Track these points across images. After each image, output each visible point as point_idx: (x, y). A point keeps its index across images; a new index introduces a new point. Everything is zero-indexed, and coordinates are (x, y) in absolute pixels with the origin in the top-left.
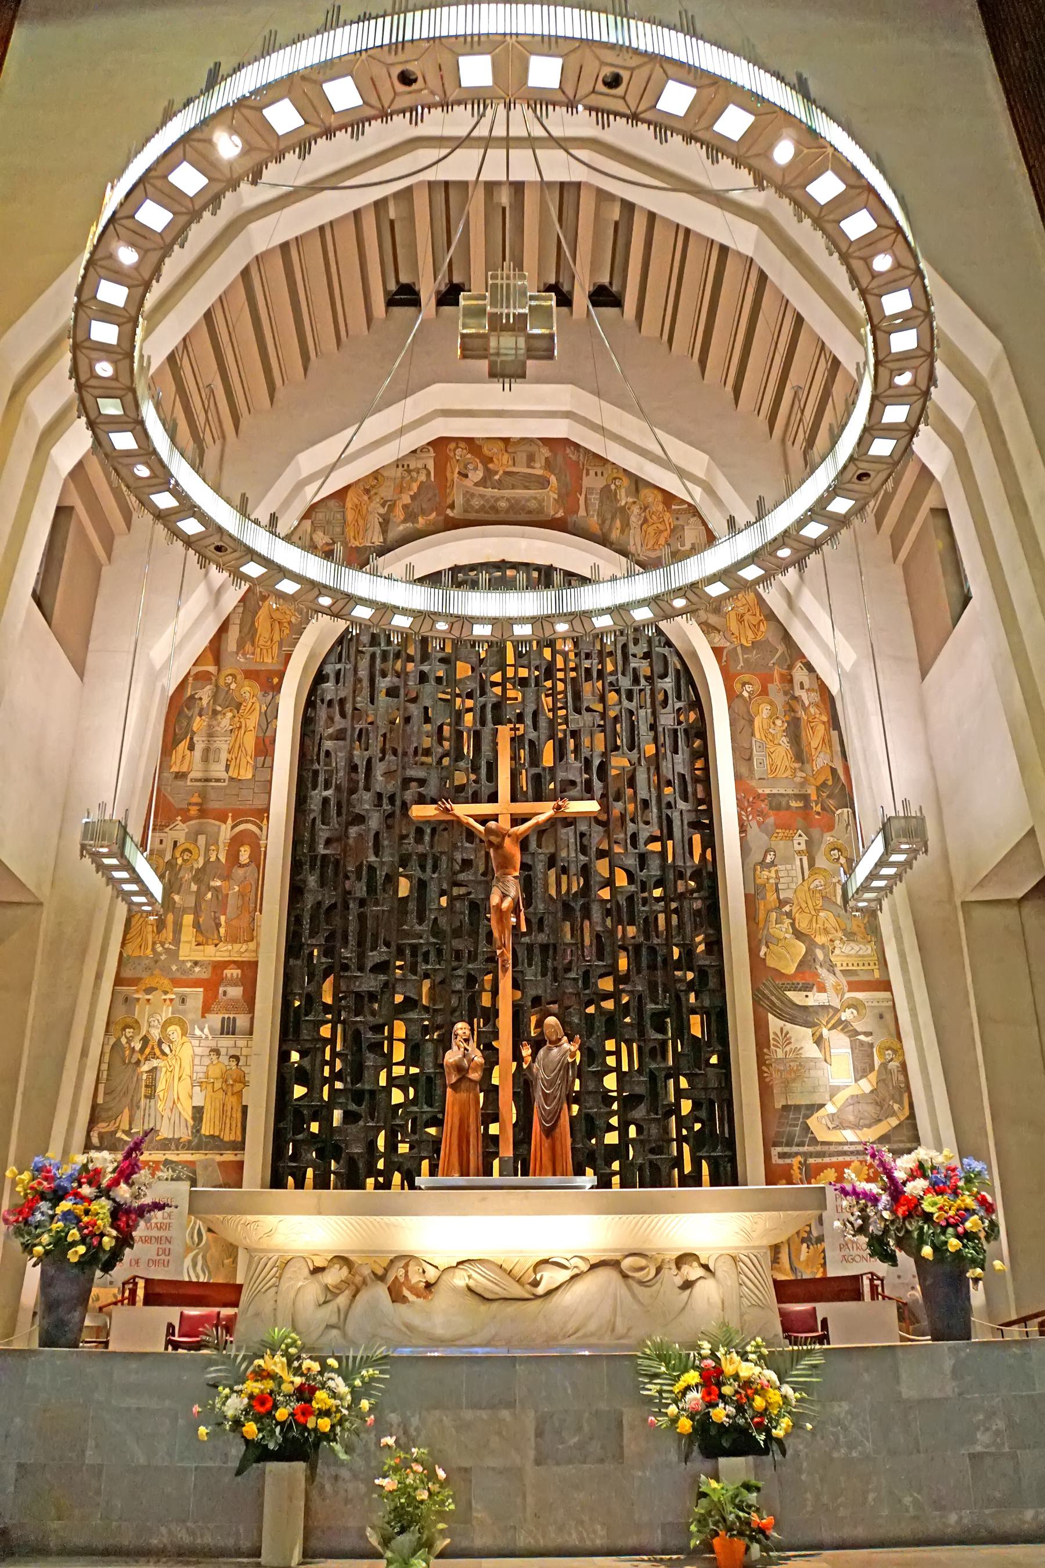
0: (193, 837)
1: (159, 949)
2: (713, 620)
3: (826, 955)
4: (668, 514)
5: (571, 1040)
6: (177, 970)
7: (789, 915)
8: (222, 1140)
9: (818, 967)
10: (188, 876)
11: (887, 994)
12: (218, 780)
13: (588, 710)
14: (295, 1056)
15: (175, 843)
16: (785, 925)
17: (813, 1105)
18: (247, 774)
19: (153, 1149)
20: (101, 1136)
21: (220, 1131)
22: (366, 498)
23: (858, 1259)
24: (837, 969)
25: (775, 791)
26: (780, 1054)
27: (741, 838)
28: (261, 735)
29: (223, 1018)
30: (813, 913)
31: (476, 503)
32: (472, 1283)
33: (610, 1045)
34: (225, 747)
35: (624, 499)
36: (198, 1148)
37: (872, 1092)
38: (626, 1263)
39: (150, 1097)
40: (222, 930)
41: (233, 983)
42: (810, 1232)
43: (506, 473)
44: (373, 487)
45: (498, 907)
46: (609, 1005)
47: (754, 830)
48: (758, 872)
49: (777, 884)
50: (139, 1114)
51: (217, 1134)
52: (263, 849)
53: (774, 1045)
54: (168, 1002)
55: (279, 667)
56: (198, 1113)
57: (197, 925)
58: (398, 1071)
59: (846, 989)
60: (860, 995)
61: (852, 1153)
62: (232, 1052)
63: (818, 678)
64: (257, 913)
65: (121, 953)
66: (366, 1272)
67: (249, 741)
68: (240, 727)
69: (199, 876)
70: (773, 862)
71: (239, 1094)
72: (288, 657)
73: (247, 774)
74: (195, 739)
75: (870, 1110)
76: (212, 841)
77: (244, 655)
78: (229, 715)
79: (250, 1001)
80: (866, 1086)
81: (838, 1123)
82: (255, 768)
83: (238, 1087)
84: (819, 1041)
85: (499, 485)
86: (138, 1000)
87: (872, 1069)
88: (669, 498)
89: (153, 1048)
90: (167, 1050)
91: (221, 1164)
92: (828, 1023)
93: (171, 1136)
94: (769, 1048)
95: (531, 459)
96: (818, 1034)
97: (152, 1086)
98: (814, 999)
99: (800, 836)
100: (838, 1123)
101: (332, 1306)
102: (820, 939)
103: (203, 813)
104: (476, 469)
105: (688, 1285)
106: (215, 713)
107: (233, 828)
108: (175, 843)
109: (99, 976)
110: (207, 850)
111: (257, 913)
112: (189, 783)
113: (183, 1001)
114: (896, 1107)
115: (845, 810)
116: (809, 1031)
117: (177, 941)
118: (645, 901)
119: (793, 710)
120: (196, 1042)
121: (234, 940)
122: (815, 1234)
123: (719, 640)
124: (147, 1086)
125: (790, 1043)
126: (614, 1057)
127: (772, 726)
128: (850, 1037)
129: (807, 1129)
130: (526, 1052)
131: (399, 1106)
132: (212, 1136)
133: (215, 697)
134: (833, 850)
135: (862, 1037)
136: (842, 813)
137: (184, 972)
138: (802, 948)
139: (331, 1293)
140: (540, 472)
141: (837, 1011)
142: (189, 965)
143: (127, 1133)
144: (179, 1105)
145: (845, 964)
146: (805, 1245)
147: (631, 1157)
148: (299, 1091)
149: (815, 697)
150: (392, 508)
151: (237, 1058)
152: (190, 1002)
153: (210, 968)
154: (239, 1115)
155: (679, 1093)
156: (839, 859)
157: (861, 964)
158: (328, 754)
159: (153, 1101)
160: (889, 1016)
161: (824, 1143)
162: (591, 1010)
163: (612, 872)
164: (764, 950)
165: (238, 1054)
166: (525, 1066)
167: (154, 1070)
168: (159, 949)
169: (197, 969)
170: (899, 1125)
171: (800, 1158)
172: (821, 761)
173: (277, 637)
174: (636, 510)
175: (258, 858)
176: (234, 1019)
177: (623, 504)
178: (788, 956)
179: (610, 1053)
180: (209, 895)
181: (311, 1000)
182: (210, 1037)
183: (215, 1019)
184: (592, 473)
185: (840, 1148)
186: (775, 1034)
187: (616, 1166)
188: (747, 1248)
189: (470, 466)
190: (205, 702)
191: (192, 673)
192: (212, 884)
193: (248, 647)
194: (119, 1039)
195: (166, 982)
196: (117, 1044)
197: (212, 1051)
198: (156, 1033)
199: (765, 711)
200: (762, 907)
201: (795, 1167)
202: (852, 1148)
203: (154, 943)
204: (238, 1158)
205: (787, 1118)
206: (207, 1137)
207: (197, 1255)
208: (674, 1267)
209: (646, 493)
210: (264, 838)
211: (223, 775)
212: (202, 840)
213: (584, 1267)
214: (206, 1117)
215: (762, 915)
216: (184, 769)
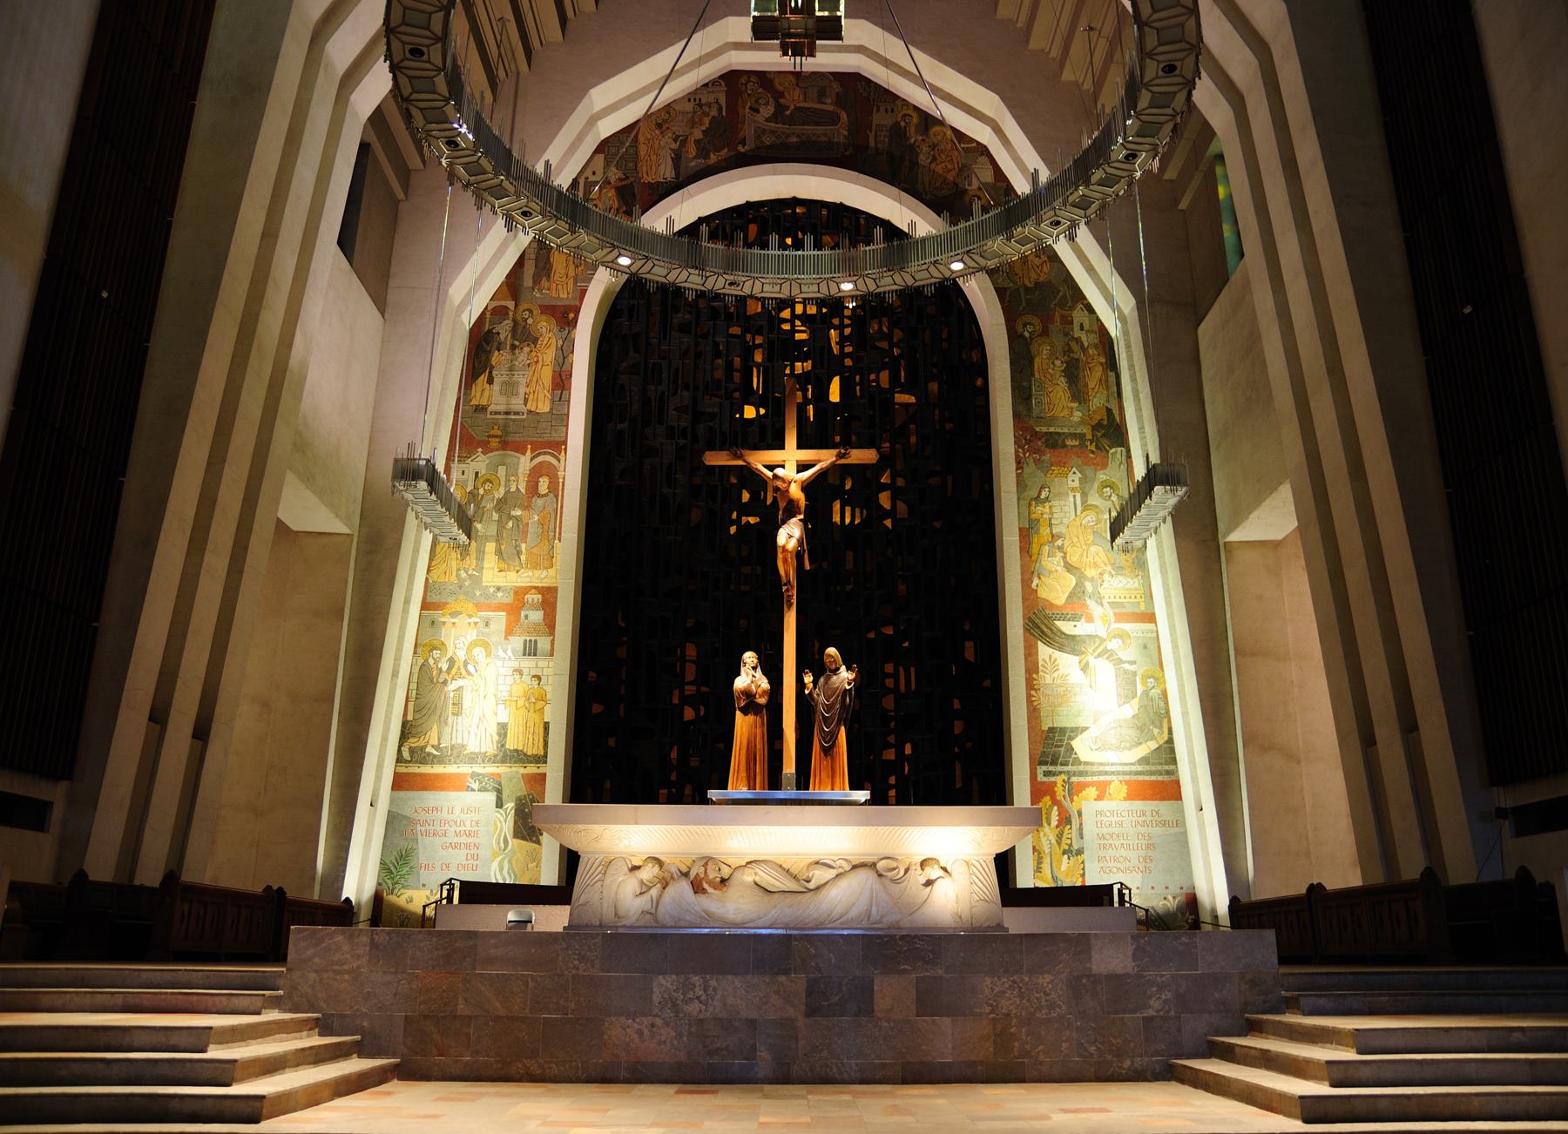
0: (494, 467)
1: (464, 575)
3: (1095, 588)
5: (848, 669)
6: (481, 595)
7: (1060, 548)
8: (525, 755)
9: (1086, 598)
10: (490, 506)
11: (1151, 626)
12: (517, 413)
13: (875, 347)
15: (477, 473)
16: (1057, 559)
17: (1077, 728)
18: (544, 407)
19: (461, 761)
20: (412, 751)
21: (524, 745)
22: (658, 132)
23: (1114, 870)
24: (1105, 601)
25: (1052, 430)
26: (1048, 679)
27: (1018, 475)
28: (558, 369)
29: (526, 640)
30: (1084, 547)
31: (768, 140)
32: (757, 879)
33: (889, 668)
34: (523, 381)
36: (503, 761)
37: (1134, 716)
38: (880, 865)
40: (523, 557)
41: (534, 607)
42: (1071, 845)
43: (796, 108)
44: (665, 121)
45: (784, 547)
46: (889, 631)
47: (1030, 468)
48: (1033, 508)
49: (1050, 520)
50: (447, 730)
51: (520, 748)
52: (561, 480)
53: (1043, 671)
54: (472, 625)
56: (503, 729)
57: (499, 553)
58: (690, 690)
59: (1113, 620)
61: (1113, 773)
62: (533, 673)
63: (1098, 320)
64: (557, 541)
65: (427, 579)
66: (674, 870)
67: (547, 375)
68: (537, 361)
69: (501, 505)
70: (1047, 498)
72: (583, 293)
73: (544, 407)
74: (494, 373)
75: (1130, 733)
76: (512, 472)
77: (540, 290)
78: (527, 349)
79: (550, 624)
80: (1131, 709)
82: (553, 401)
83: (540, 705)
85: (791, 121)
86: (444, 623)
87: (1134, 696)
89: (459, 669)
90: (470, 668)
91: (522, 775)
92: (1094, 651)
93: (477, 750)
94: (1037, 673)
95: (822, 93)
96: (1084, 661)
97: (458, 704)
99: (1074, 473)
101: (646, 897)
102: (1090, 573)
103: (505, 445)
104: (767, 104)
105: (929, 883)
106: (513, 347)
107: (532, 460)
108: (477, 473)
109: (407, 602)
110: (508, 480)
111: (557, 541)
112: (489, 416)
113: (487, 624)
114: (1156, 731)
115: (1119, 449)
116: (1075, 659)
117: (480, 569)
119: (1071, 350)
120: (499, 663)
121: (535, 566)
122: (1076, 847)
124: (453, 704)
125: (1057, 669)
126: (892, 680)
127: (1052, 366)
128: (1114, 665)
130: (808, 679)
131: (690, 722)
132: (517, 751)
133: (514, 331)
134: (1106, 487)
135: (1126, 666)
136: (1116, 452)
137: (487, 597)
138: (1072, 580)
139: (645, 888)
140: (831, 108)
141: (1103, 640)
142: (492, 590)
143: (436, 748)
144: (485, 722)
145: (1112, 597)
146: (1066, 856)
147: (906, 772)
148: (597, 708)
149: (1094, 338)
150: (684, 143)
151: (539, 678)
152: (493, 626)
153: (512, 594)
154: (542, 730)
156: (1110, 496)
157: (1127, 596)
158: (622, 387)
159: (459, 717)
160: (1152, 650)
161: (1086, 763)
162: (872, 635)
163: (894, 505)
164: (1036, 581)
165: (540, 674)
166: (807, 692)
167: (460, 689)
168: (464, 575)
169: (500, 594)
170: (1158, 748)
171: (1063, 777)
172: (1098, 401)
173: (572, 273)
174: (925, 149)
175: (555, 489)
176: (536, 642)
177: (913, 140)
178: (1058, 587)
179: (888, 676)
180: (510, 524)
182: (513, 658)
184: (882, 109)
185: (1102, 768)
186: (1043, 660)
187: (892, 780)
188: (977, 855)
189: (762, 101)
190: (502, 337)
191: (489, 308)
192: (513, 513)
193: (544, 283)
194: (427, 660)
195: (471, 606)
196: (424, 668)
197: (514, 671)
198: (461, 655)
199: (1045, 352)
200: (1035, 540)
201: (1059, 785)
202: (1113, 769)
203: (458, 570)
204: (541, 771)
205: (1053, 739)
206: (510, 751)
207: (503, 860)
208: (919, 868)
210: (562, 469)
211: (522, 408)
212: (502, 471)
213: (847, 867)
215: (1035, 548)
216: (484, 402)
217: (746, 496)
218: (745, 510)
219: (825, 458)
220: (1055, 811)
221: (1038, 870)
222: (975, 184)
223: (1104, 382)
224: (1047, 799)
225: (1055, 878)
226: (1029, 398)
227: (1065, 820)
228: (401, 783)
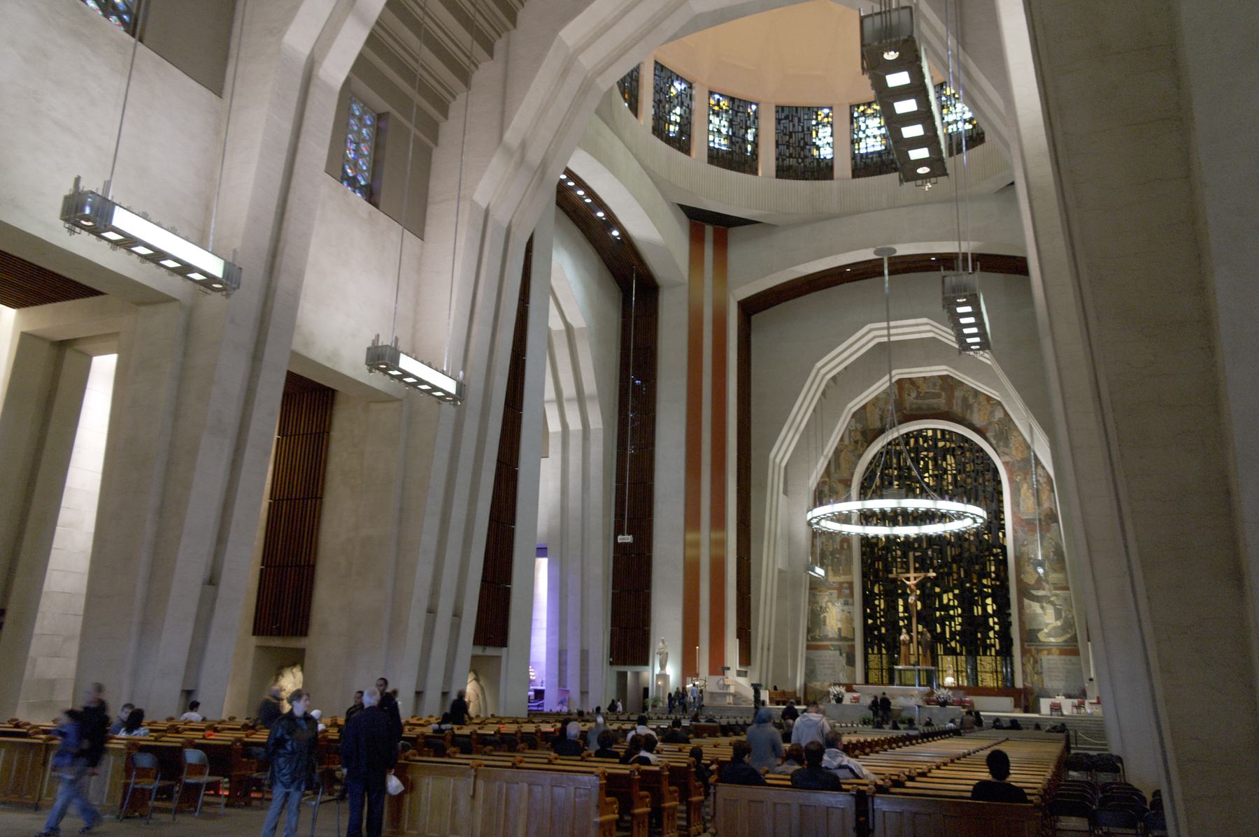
2: (1006, 450)
4: (988, 406)
11: (1067, 592)
14: (868, 611)
26: (1028, 611)
31: (914, 406)
35: (971, 400)
39: (825, 624)
43: (926, 393)
55: (850, 478)
56: (839, 629)
57: (833, 570)
60: (1058, 592)
63: (1047, 472)
71: (851, 624)
72: (852, 475)
79: (852, 594)
80: (1059, 623)
81: (1049, 635)
84: (1042, 608)
85: (924, 398)
87: (1061, 617)
88: (989, 398)
97: (825, 621)
98: (1040, 593)
100: (1049, 635)
114: (1070, 631)
116: (1038, 604)
118: (982, 557)
121: (845, 574)
123: (1007, 459)
129: (1037, 637)
140: (938, 391)
148: (870, 621)
149: (1045, 480)
151: (850, 612)
155: (995, 623)
167: (825, 617)
172: (1046, 505)
181: (872, 591)
183: (842, 600)
198: (824, 605)
209: (982, 399)
212: (831, 541)
214: (842, 632)
217: (916, 545)
218: (915, 550)
219: (922, 575)
220: (1032, 662)
221: (1024, 680)
222: (996, 420)
223: (1049, 498)
224: (1028, 655)
225: (1032, 683)
226: (1018, 506)
227: (1036, 662)
228: (808, 647)
